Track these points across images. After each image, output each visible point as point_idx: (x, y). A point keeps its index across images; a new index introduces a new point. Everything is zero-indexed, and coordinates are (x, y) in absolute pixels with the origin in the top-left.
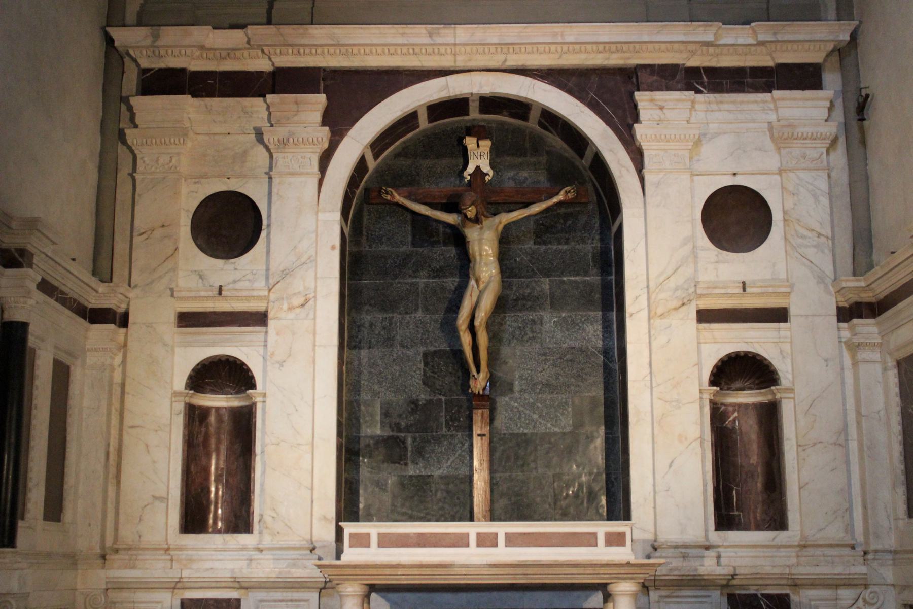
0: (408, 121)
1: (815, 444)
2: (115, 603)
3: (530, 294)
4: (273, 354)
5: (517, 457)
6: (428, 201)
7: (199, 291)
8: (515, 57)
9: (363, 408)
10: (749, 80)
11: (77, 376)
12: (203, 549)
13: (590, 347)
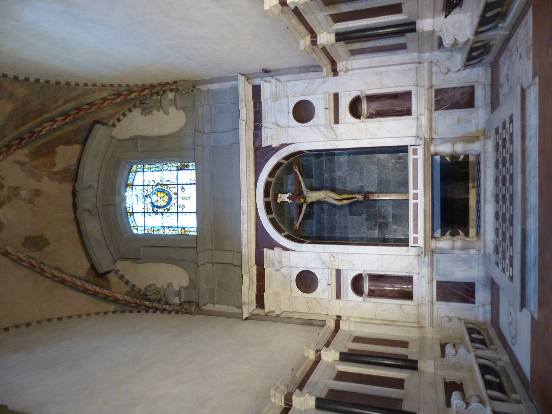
0: (272, 221)
1: (381, 82)
2: (438, 324)
3: (330, 180)
4: (350, 267)
5: (386, 184)
6: (299, 214)
7: (329, 292)
8: (251, 186)
9: (369, 237)
10: (258, 109)
11: (358, 334)
12: (418, 293)
13: (347, 160)
